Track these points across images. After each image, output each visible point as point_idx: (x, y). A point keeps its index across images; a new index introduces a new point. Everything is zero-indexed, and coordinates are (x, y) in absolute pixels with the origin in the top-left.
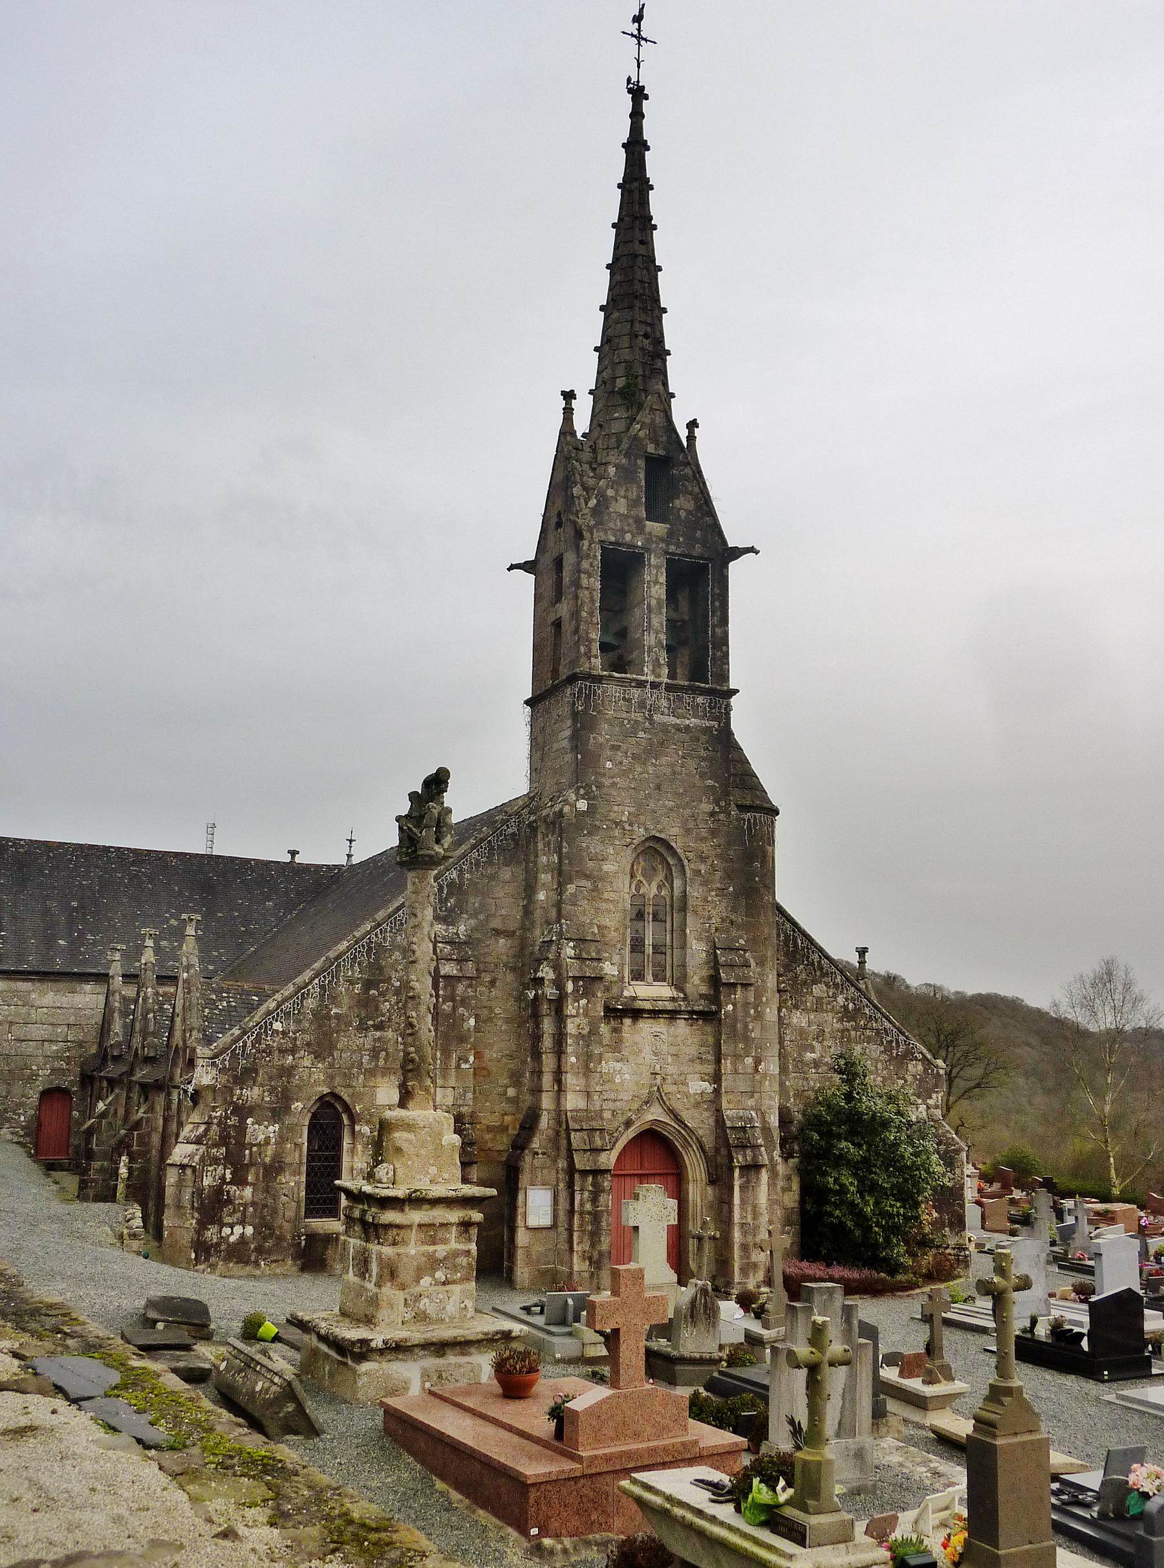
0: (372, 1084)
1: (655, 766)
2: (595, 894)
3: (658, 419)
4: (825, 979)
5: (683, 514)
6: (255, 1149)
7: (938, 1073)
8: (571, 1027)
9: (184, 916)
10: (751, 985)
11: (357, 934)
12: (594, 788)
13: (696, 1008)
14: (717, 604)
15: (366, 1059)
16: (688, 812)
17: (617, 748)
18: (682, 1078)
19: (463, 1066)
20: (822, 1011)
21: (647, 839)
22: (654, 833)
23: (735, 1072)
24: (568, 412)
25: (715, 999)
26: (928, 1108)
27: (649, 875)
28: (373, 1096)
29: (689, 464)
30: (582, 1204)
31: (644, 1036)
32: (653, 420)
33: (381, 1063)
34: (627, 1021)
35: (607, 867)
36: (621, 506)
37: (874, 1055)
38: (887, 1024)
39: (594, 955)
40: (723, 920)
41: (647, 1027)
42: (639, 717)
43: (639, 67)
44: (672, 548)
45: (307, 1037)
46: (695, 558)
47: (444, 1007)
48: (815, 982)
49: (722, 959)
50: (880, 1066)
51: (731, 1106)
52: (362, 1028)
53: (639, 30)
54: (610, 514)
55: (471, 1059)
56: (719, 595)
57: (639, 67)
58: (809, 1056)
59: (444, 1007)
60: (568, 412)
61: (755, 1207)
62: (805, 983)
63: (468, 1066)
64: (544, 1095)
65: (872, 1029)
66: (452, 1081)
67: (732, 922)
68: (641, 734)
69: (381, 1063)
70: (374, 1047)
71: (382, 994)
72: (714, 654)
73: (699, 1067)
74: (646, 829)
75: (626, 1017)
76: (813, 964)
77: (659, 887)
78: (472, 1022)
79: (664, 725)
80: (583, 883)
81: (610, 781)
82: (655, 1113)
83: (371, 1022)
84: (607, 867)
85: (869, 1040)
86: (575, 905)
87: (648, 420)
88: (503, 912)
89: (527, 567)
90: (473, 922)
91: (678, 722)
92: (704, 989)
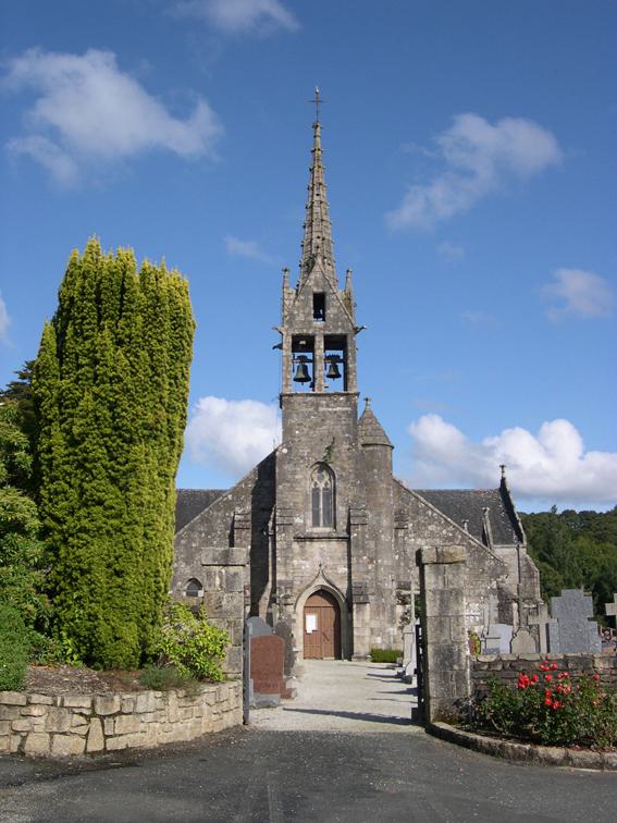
23: (358, 563)
40: (355, 496)
41: (316, 545)
42: (311, 409)
44: (327, 332)
79: (324, 412)
82: (321, 582)
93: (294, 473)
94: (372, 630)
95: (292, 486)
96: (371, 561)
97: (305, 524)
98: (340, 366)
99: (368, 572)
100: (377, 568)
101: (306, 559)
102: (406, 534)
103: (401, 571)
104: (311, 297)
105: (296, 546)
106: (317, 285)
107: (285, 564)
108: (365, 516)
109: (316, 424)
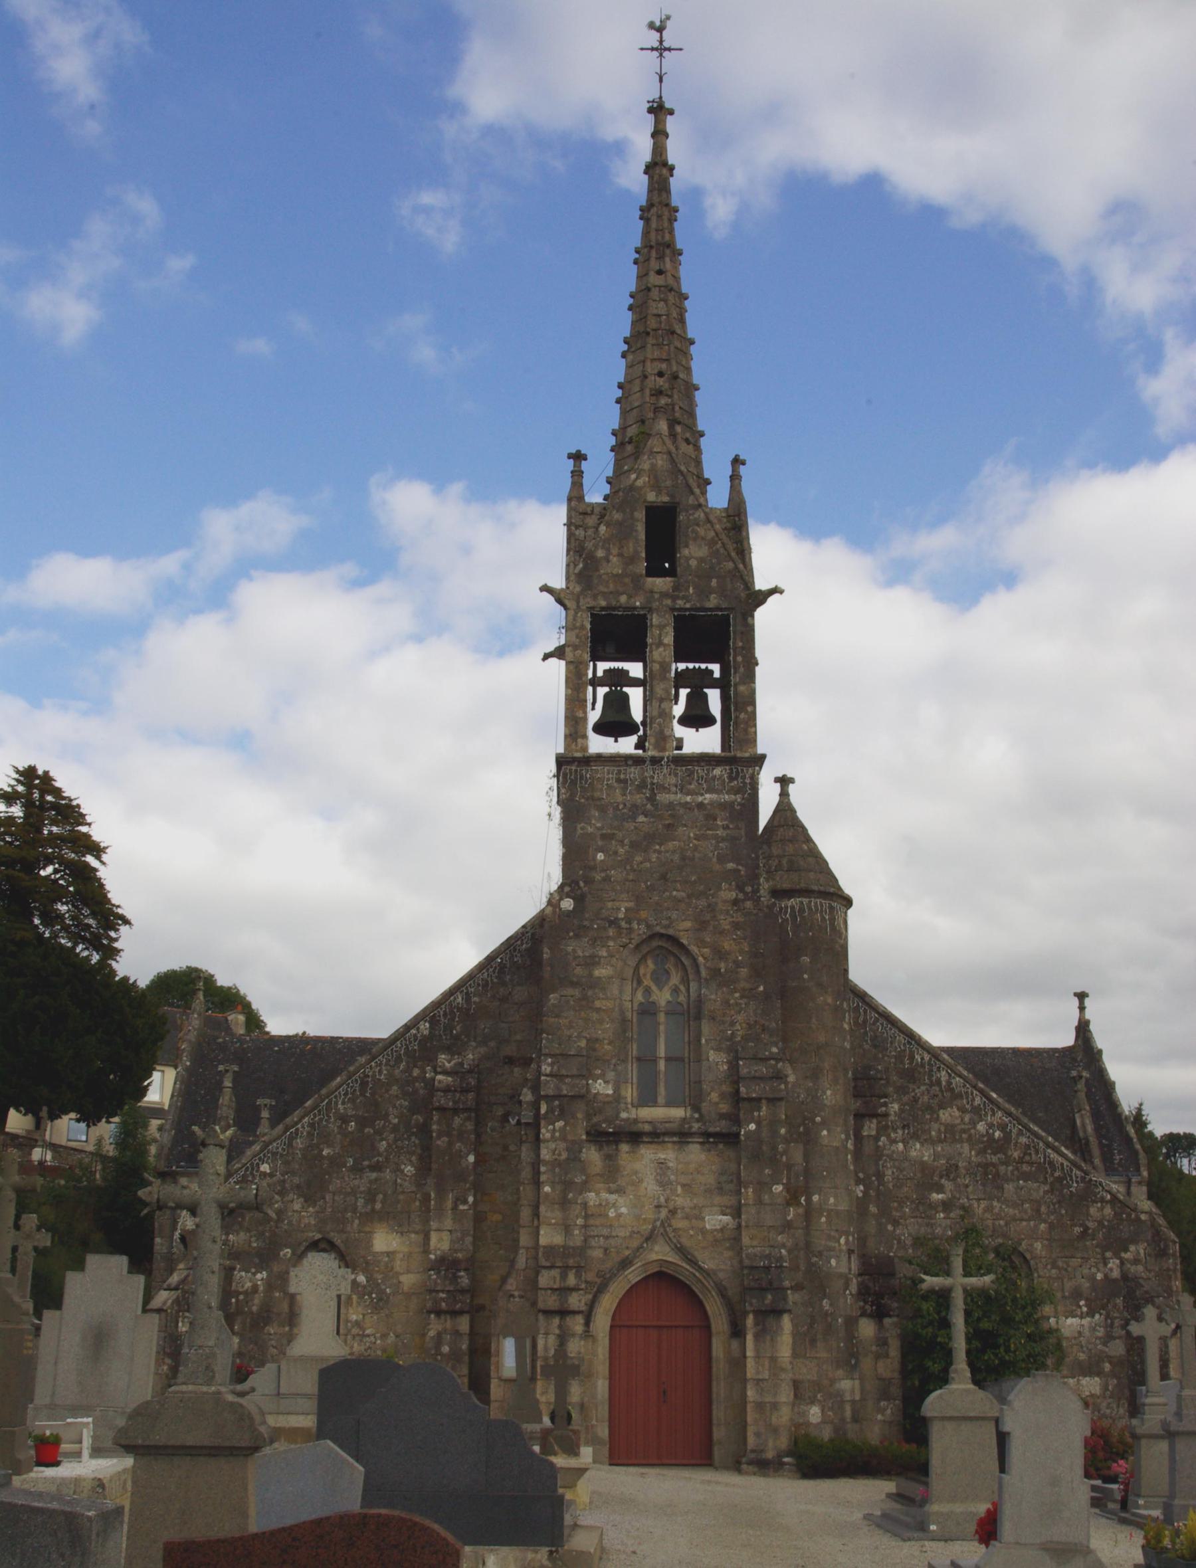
0: (367, 1229)
1: (659, 852)
2: (584, 1003)
3: (660, 462)
4: (959, 1102)
5: (693, 563)
6: (241, 1297)
7: (1138, 1219)
8: (545, 1154)
9: (221, 1068)
10: (781, 1099)
11: (351, 1069)
12: (582, 884)
13: (711, 1130)
14: (739, 659)
15: (361, 1202)
16: (702, 903)
17: (611, 837)
18: (696, 1212)
19: (461, 1207)
20: (955, 1141)
21: (652, 937)
22: (658, 929)
23: (759, 1202)
24: (577, 474)
25: (736, 1120)
26: (1122, 1263)
27: (660, 978)
28: (369, 1244)
29: (700, 505)
30: (546, 1349)
31: (643, 1162)
32: (653, 466)
33: (378, 1206)
34: (624, 1147)
35: (600, 972)
36: (615, 566)
37: (1035, 1195)
38: (1053, 1156)
39: (575, 1072)
40: (750, 1026)
41: (648, 1155)
42: (639, 798)
43: (661, 80)
44: (680, 603)
45: (296, 1180)
46: (710, 610)
47: (439, 1142)
48: (942, 1106)
49: (744, 1071)
50: (1043, 1209)
51: (755, 1243)
52: (357, 1169)
53: (661, 42)
54: (600, 576)
55: (471, 1199)
56: (743, 648)
57: (661, 80)
58: (936, 1197)
59: (439, 1142)
60: (577, 474)
61: (773, 1359)
62: (929, 1108)
63: (466, 1207)
64: (522, 1231)
65: (1030, 1163)
66: (448, 1223)
67: (764, 1029)
68: (641, 819)
69: (378, 1206)
70: (369, 1189)
71: (379, 1132)
72: (737, 717)
73: (717, 1199)
74: (648, 926)
75: (621, 1141)
76: (939, 1082)
77: (676, 990)
78: (471, 1158)
79: (671, 806)
80: (570, 991)
81: (603, 875)
82: (660, 1252)
83: (366, 1163)
84: (600, 972)
85: (1026, 1177)
86: (557, 1016)
87: (646, 466)
88: (518, 1037)
89: (559, 653)
90: (482, 1050)
91: (688, 799)
92: (724, 1108)
93: (592, 962)
94: (796, 1385)
95: (584, 997)
96: (792, 1197)
97: (617, 1098)
98: (714, 697)
99: (787, 1226)
100: (809, 1214)
101: (620, 1191)
102: (883, 1130)
103: (871, 1227)
104: (641, 515)
105: (593, 1156)
106: (656, 487)
107: (564, 1203)
108: (779, 1077)
109: (651, 838)
